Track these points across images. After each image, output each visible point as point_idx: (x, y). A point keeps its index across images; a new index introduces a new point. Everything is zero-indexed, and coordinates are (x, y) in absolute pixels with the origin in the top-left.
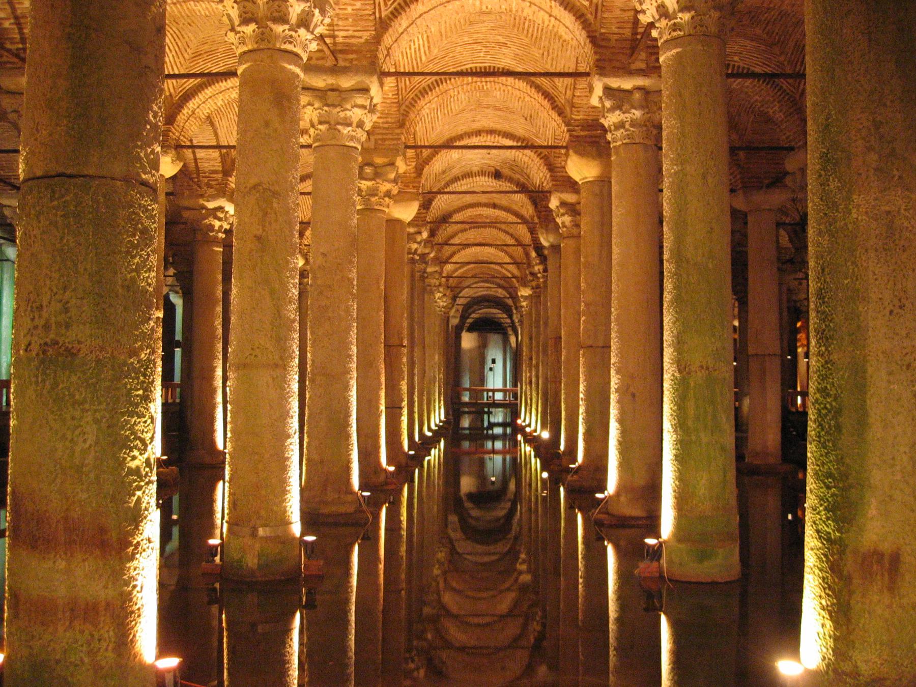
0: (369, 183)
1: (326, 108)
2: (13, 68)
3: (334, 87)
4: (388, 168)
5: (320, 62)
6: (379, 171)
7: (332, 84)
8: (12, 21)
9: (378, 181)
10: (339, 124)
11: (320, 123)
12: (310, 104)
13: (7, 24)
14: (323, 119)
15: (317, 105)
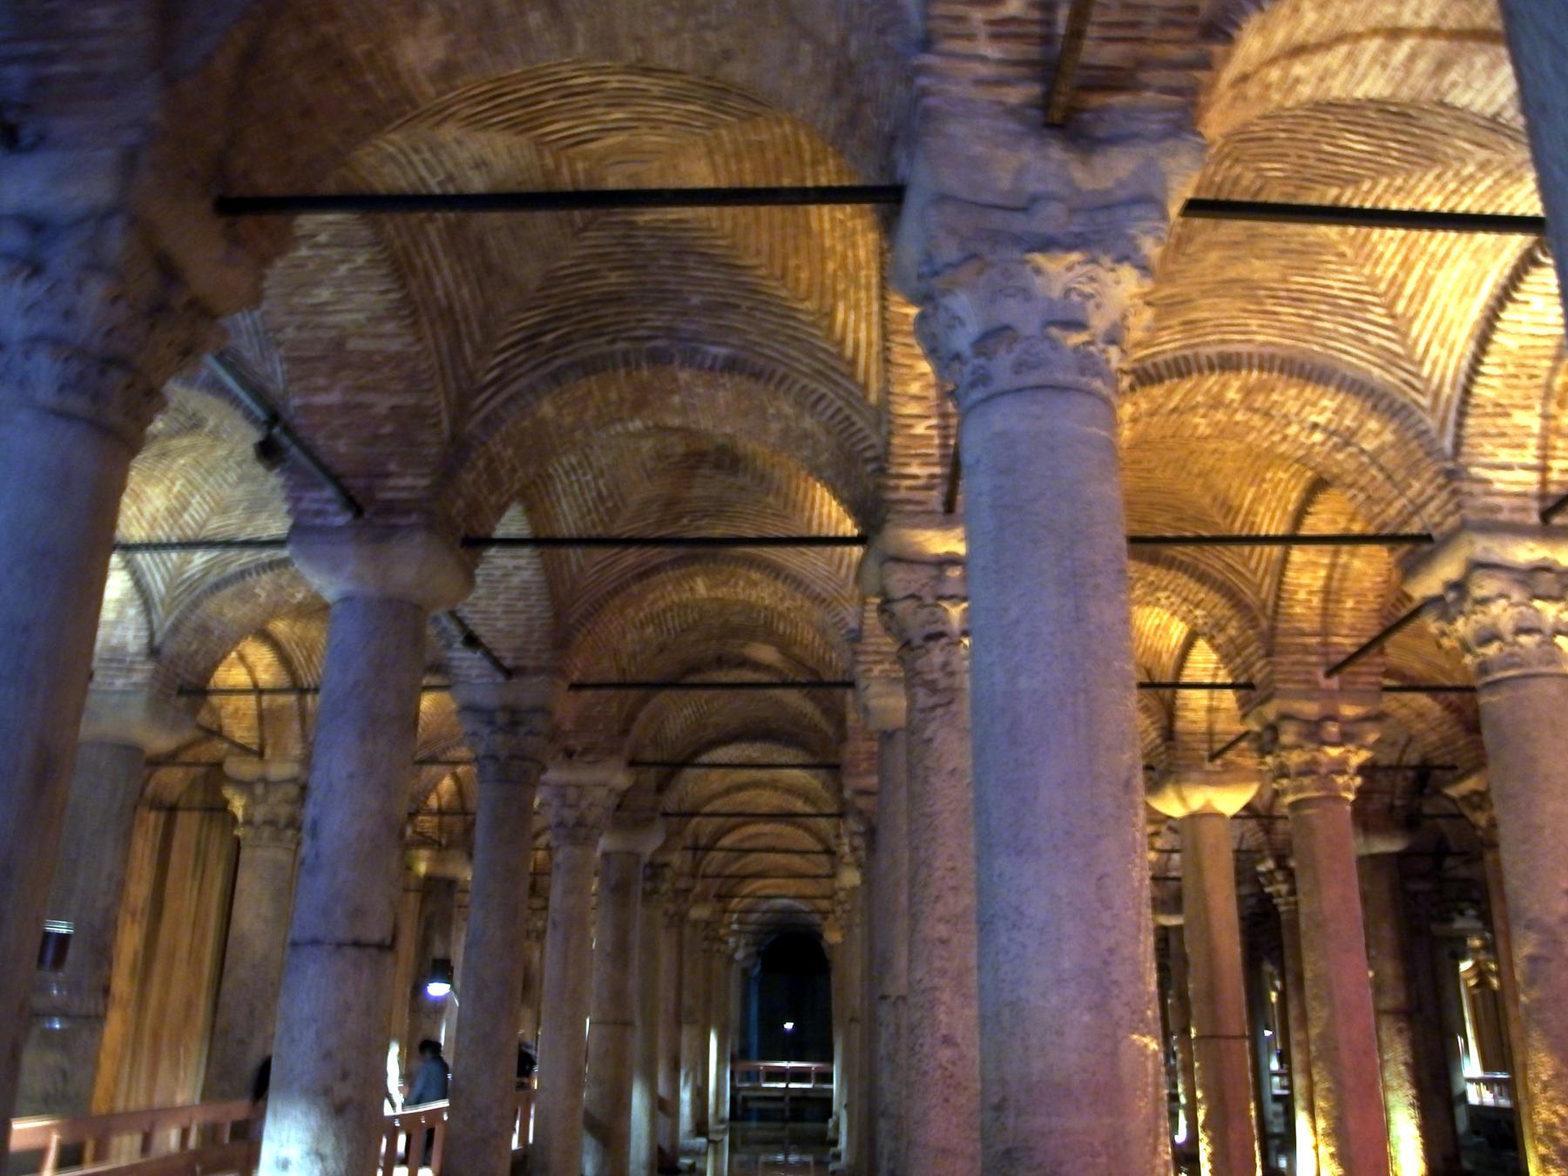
0: (1334, 752)
1: (1538, 604)
2: (917, 514)
3: (1546, 564)
4: (1368, 726)
5: (1517, 517)
6: (1348, 729)
7: (1545, 559)
8: (933, 422)
9: (1351, 747)
10: (1559, 632)
11: (1528, 631)
12: (1502, 596)
13: (920, 429)
14: (1527, 624)
15: (1516, 596)
